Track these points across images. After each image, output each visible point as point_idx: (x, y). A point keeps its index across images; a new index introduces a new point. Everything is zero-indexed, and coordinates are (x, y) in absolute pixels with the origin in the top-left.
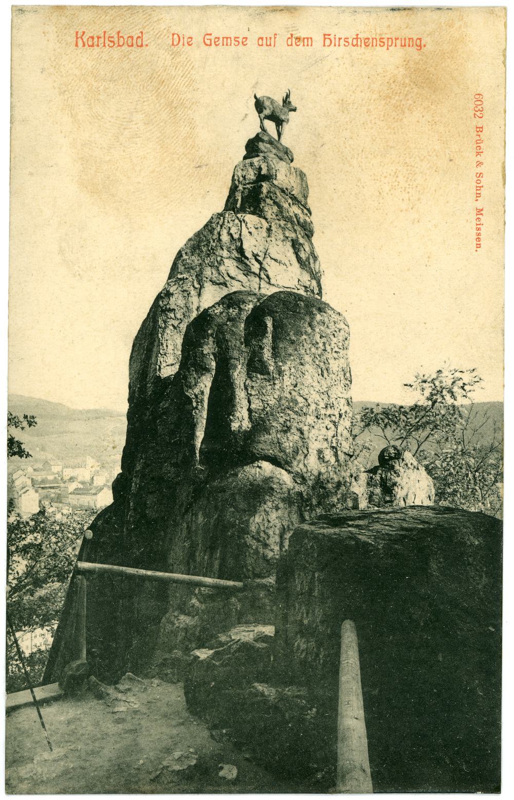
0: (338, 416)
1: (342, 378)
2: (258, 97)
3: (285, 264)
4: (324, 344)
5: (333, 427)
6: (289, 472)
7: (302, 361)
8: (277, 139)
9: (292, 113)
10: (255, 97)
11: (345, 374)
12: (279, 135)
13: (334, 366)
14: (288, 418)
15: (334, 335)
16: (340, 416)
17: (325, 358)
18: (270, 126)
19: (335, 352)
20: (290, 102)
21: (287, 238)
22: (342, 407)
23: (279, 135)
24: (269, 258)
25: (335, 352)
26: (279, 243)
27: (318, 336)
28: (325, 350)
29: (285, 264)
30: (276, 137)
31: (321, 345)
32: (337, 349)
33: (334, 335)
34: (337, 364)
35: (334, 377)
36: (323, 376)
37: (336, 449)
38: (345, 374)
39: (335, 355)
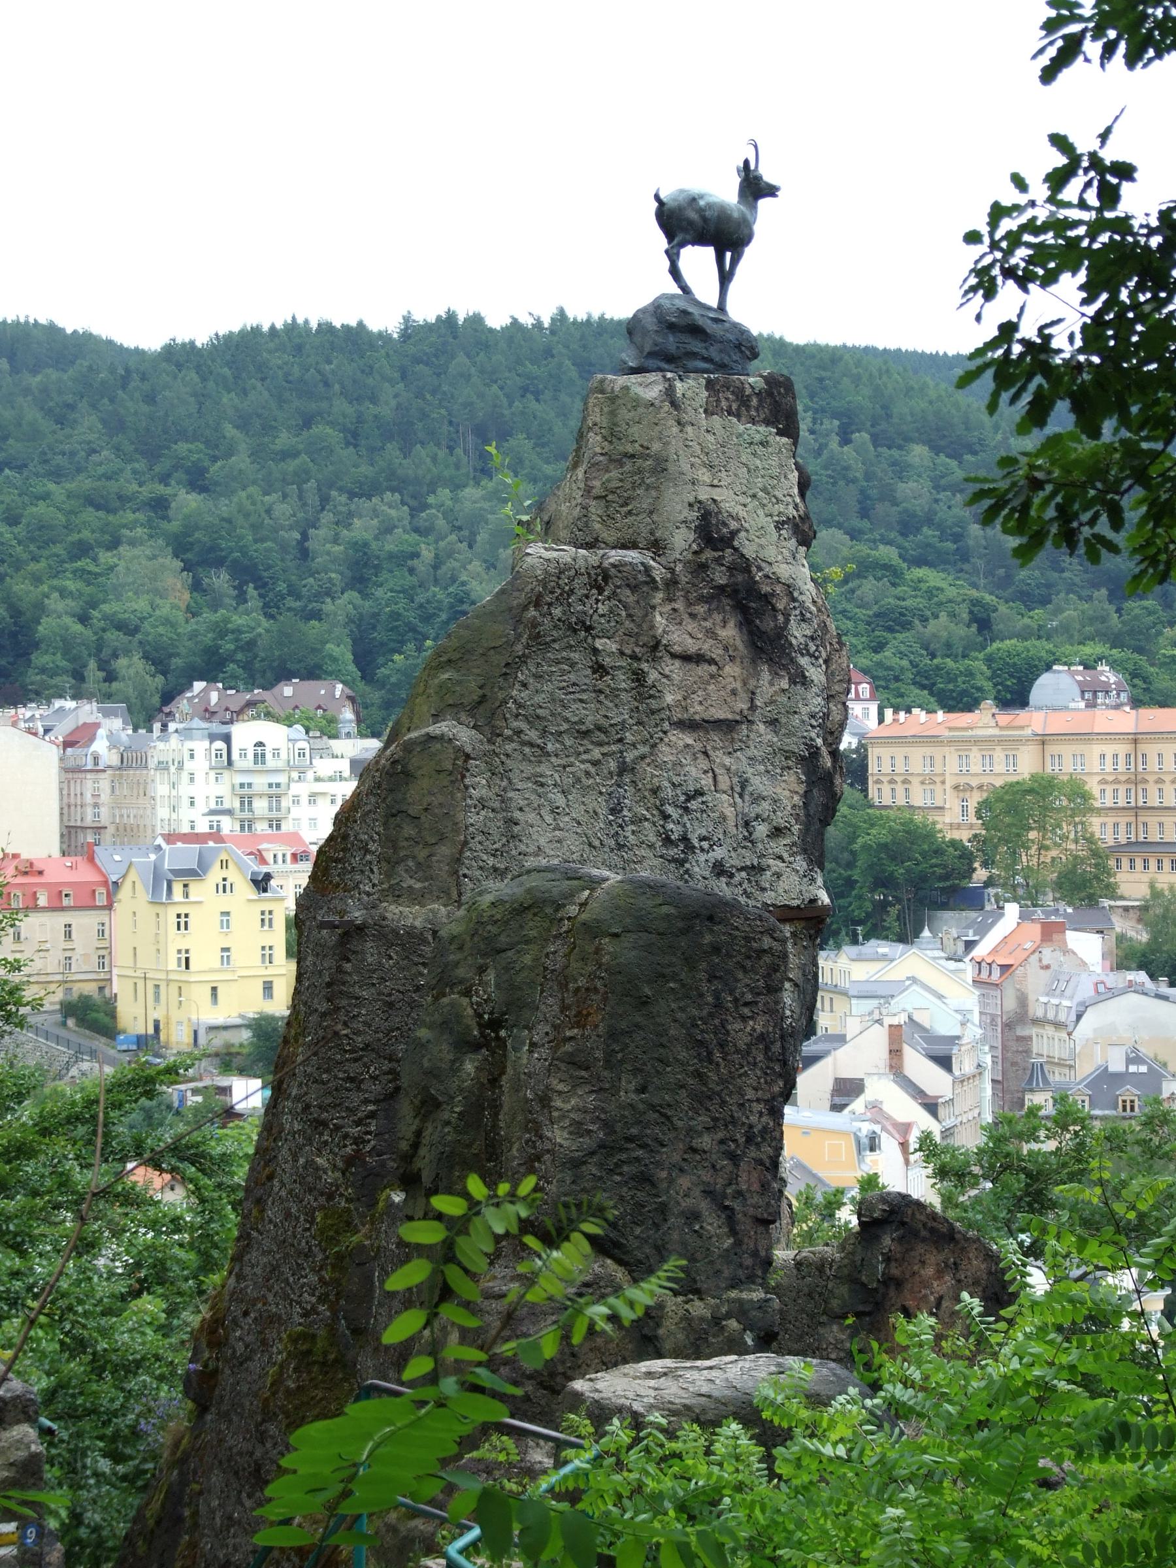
0: (742, 1140)
1: (760, 1057)
2: (662, 196)
3: (711, 661)
4: (717, 995)
5: (730, 1168)
6: (620, 1262)
7: (664, 1040)
8: (713, 302)
9: (764, 204)
11: (767, 1048)
12: (725, 278)
13: (742, 1031)
14: (624, 1156)
15: (743, 967)
16: (750, 1139)
17: (717, 1022)
19: (746, 1004)
20: (758, 178)
21: (721, 589)
22: (754, 1119)
23: (725, 278)
24: (667, 659)
25: (746, 1004)
26: (701, 609)
27: (703, 975)
28: (718, 1005)
29: (711, 661)
31: (710, 999)
32: (749, 997)
33: (743, 967)
34: (748, 1029)
35: (736, 1057)
36: (711, 1062)
37: (732, 1210)
38: (767, 1048)
39: (746, 1011)
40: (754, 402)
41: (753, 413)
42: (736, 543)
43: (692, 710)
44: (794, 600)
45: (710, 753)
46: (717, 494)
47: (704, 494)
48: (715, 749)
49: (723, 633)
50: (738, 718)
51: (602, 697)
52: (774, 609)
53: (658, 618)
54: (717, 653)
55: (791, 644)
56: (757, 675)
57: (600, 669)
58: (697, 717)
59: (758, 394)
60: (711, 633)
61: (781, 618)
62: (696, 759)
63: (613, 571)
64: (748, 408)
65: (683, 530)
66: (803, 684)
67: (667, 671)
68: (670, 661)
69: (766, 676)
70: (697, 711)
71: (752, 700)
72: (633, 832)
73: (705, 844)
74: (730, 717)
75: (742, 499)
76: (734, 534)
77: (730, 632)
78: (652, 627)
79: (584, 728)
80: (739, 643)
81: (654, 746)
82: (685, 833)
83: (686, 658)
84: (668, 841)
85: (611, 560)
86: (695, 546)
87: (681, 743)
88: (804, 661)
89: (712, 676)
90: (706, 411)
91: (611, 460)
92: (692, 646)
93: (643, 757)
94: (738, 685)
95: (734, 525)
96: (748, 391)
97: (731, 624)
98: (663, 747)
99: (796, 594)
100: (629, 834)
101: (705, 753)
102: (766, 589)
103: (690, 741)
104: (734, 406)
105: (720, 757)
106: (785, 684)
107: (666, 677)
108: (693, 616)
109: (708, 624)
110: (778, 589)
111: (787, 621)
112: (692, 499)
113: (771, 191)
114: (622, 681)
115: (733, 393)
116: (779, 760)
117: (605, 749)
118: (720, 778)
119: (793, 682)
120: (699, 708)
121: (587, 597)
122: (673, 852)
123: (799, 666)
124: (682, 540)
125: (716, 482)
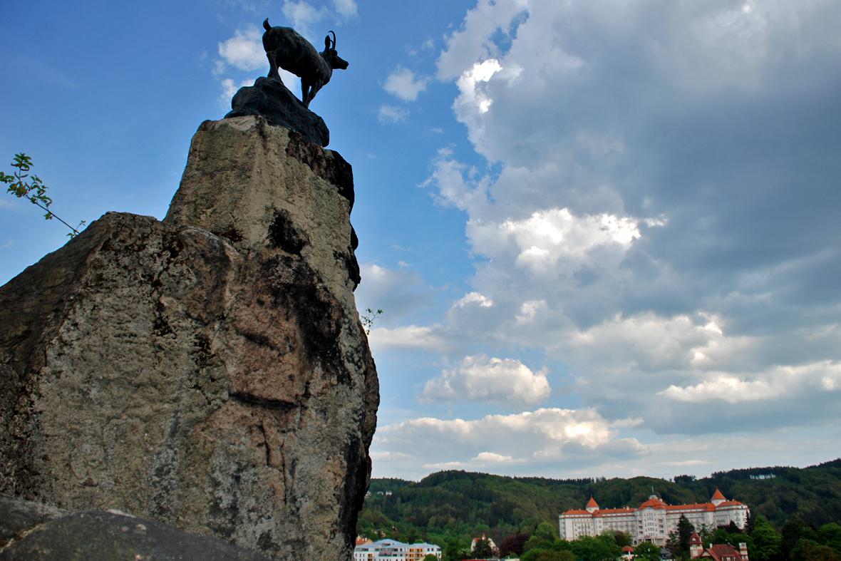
9: (337, 73)
10: (266, 25)
12: (308, 97)
18: (291, 81)
26: (268, 299)
30: (300, 96)
40: (324, 163)
41: (322, 170)
42: (303, 252)
43: (252, 386)
44: (344, 316)
45: (266, 428)
46: (290, 208)
47: (281, 205)
48: (270, 425)
49: (285, 325)
50: (293, 401)
51: (161, 354)
52: (329, 317)
53: (228, 293)
54: (279, 340)
55: (340, 351)
56: (312, 369)
57: (161, 326)
58: (256, 393)
59: (328, 160)
60: (274, 321)
61: (334, 327)
62: (251, 432)
63: (190, 241)
64: (319, 165)
65: (259, 227)
66: (349, 384)
67: (232, 343)
68: (235, 336)
69: (318, 370)
70: (258, 388)
71: (307, 388)
72: (179, 497)
73: (254, 515)
74: (287, 399)
75: (311, 223)
76: (302, 244)
77: (290, 326)
78: (221, 299)
79: (137, 381)
80: (298, 337)
81: (211, 412)
82: (235, 502)
83: (250, 337)
84: (215, 509)
85: (189, 231)
86: (268, 242)
87: (239, 414)
88: (350, 367)
89: (273, 359)
90: (287, 150)
91: (204, 174)
92: (258, 328)
93: (198, 421)
94: (295, 373)
95: (302, 237)
96: (320, 153)
97: (294, 319)
98: (220, 414)
99: (346, 312)
100: (175, 497)
101: (261, 428)
102: (323, 298)
103: (248, 414)
104: (309, 159)
105: (272, 433)
106: (334, 380)
107: (230, 348)
108: (261, 303)
109: (275, 313)
110: (334, 303)
111: (338, 331)
112: (269, 204)
113: (343, 65)
114: (185, 341)
115: (309, 149)
116: (327, 444)
117: (158, 406)
118: (273, 453)
119: (340, 380)
120: (259, 386)
121: (159, 255)
122: (221, 521)
123: (345, 370)
124: (257, 234)
125: (290, 200)
